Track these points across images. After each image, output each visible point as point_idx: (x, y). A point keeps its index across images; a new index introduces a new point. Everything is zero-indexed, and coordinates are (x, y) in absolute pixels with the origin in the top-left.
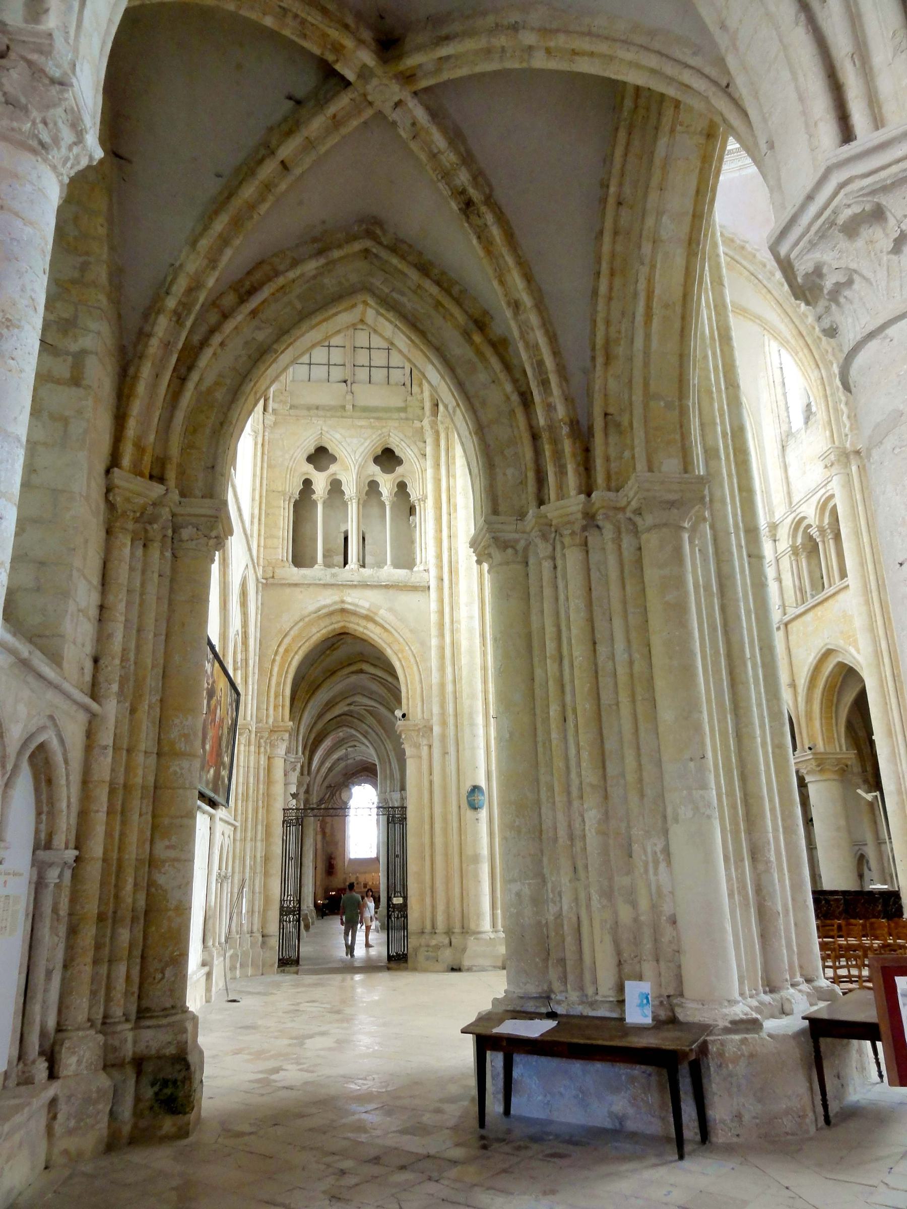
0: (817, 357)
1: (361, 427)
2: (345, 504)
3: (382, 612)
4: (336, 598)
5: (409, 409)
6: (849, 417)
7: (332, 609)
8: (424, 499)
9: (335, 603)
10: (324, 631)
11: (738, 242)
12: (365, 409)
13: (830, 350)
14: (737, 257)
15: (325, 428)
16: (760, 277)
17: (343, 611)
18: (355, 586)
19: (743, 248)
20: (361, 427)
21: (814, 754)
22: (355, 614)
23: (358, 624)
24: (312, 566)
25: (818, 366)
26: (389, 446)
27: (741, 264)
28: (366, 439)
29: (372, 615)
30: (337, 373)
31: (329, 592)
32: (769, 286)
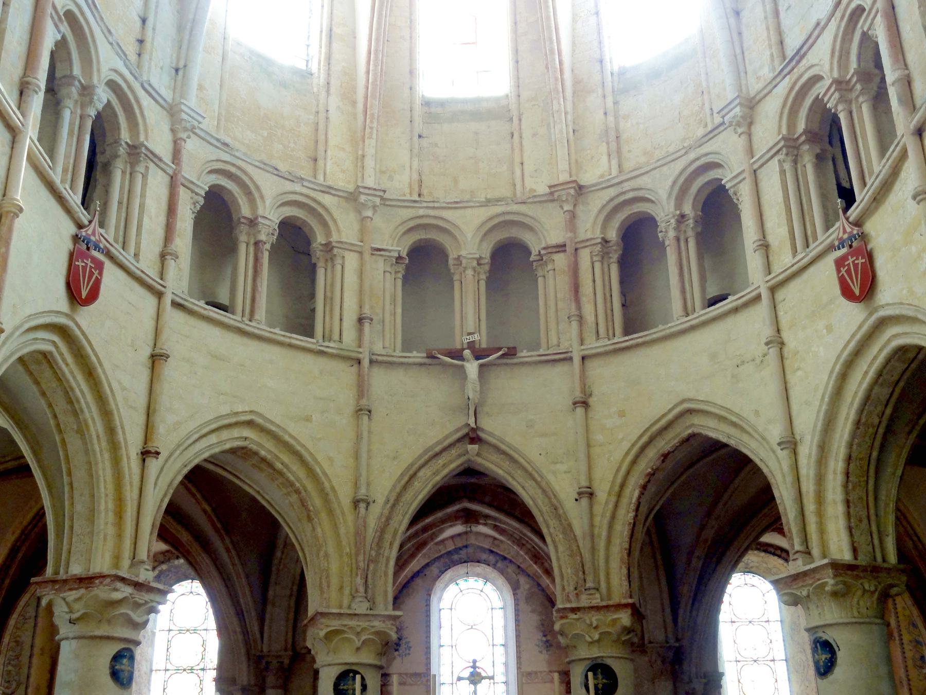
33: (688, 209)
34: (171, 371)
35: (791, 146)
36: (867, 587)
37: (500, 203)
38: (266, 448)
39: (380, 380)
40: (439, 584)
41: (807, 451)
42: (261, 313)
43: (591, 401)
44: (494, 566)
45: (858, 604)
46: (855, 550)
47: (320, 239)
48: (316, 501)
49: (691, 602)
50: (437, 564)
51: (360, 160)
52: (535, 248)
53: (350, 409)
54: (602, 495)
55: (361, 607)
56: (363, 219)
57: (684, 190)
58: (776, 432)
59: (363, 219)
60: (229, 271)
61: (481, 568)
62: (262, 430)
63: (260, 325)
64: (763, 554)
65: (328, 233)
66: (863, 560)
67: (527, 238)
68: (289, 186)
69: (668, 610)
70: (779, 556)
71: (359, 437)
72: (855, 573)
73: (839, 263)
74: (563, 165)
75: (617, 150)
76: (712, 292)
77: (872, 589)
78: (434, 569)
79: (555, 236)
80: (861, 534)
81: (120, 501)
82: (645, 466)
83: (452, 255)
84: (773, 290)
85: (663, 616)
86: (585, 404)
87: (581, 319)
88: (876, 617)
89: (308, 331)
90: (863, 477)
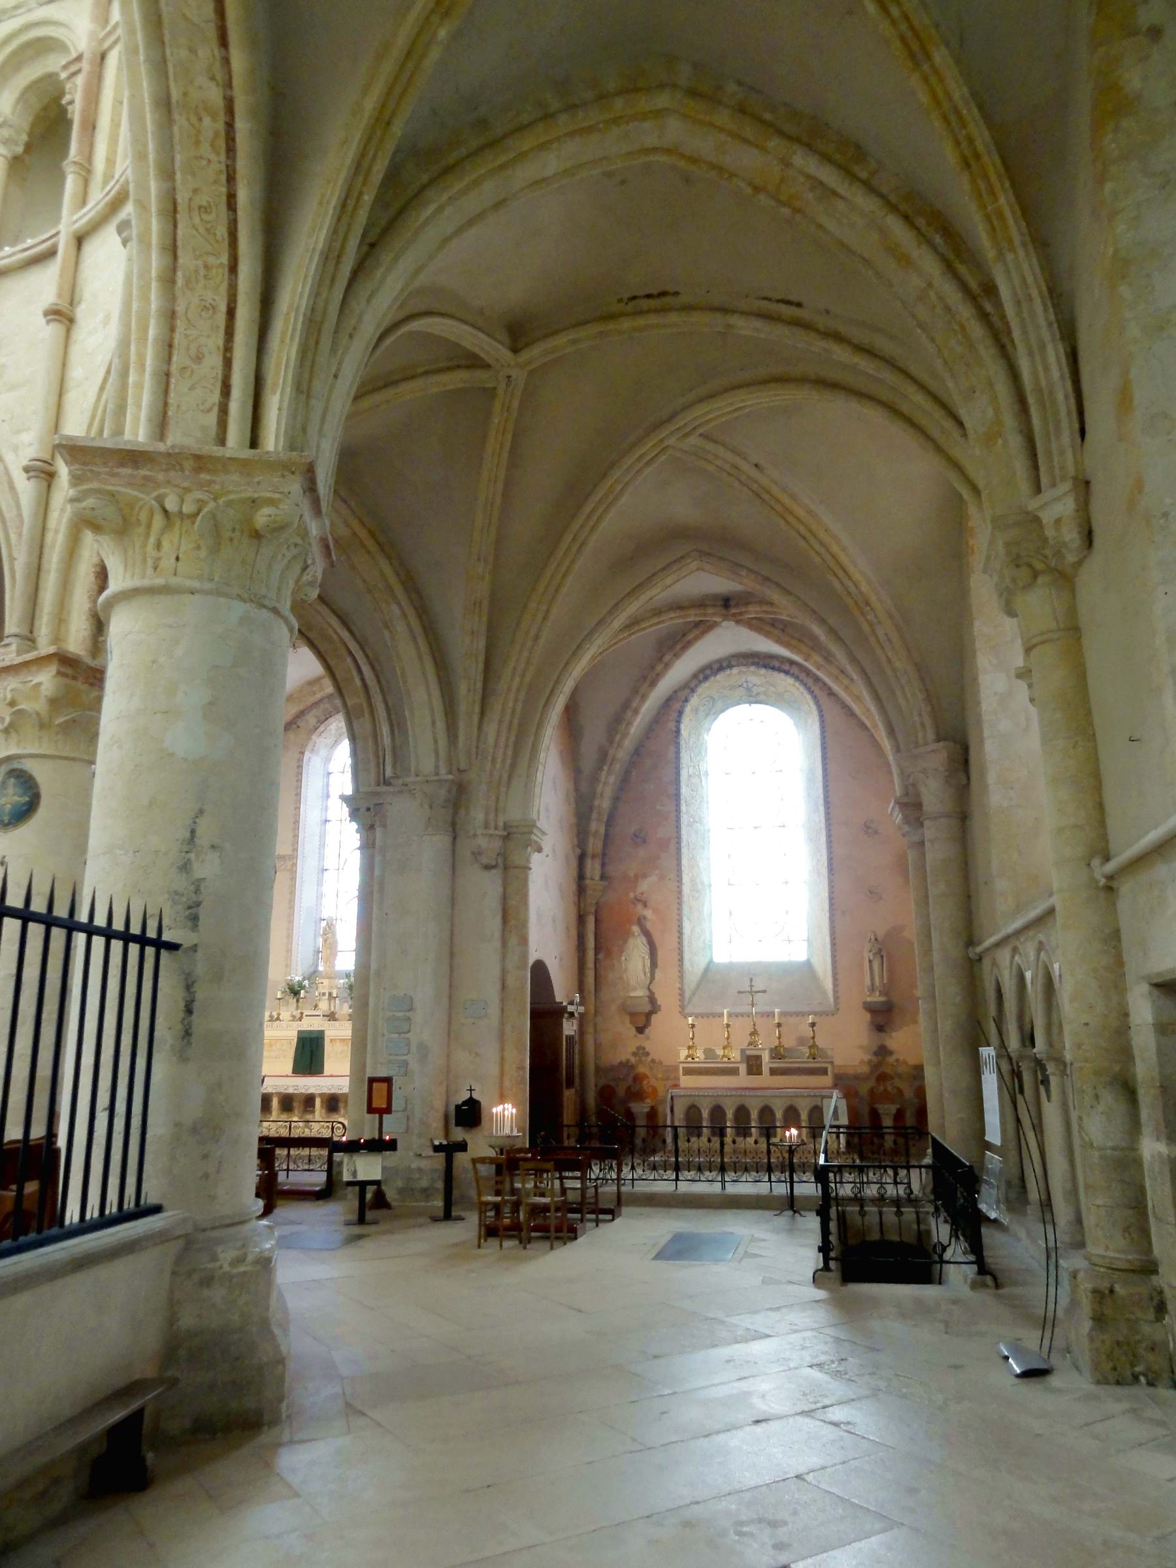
36: (171, 504)
37: (19, 11)
43: (81, 312)
45: (158, 546)
49: (477, 709)
50: (314, 711)
64: (763, 671)
69: (441, 725)
70: (787, 673)
72: (143, 472)
77: (188, 508)
78: (311, 719)
80: (191, 388)
85: (434, 733)
88: (199, 578)
90: (216, 255)
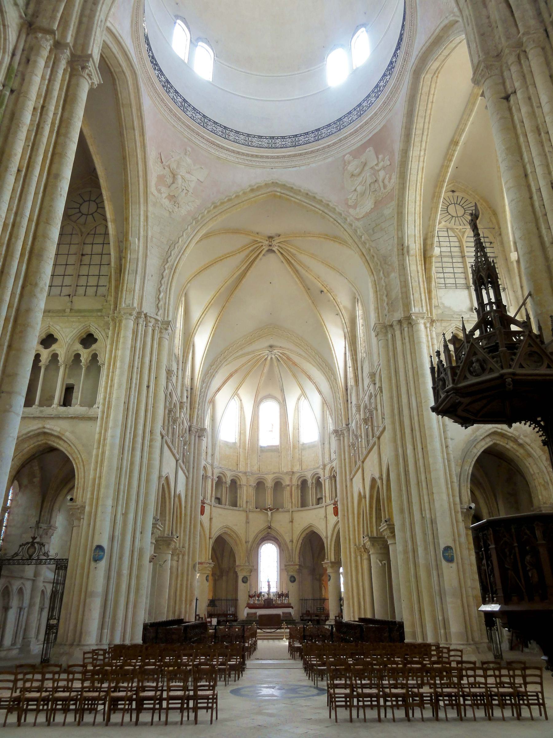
0: (372, 268)
1: (73, 322)
2: (58, 369)
3: (67, 434)
4: (40, 426)
5: (104, 310)
6: (387, 304)
7: (36, 432)
8: (104, 364)
9: (39, 429)
10: (32, 446)
11: (324, 201)
12: (79, 311)
13: (379, 264)
14: (326, 211)
15: (51, 323)
16: (339, 221)
17: (45, 433)
18: (53, 418)
19: (328, 205)
20: (73, 322)
21: (388, 525)
22: (52, 435)
23: (54, 442)
24: (31, 407)
25: (373, 273)
26: (91, 332)
27: (328, 215)
28: (75, 329)
29: (60, 435)
30: (66, 291)
31: (36, 422)
32: (345, 227)
33: (314, 481)
34: (214, 520)
35: (330, 478)
38: (229, 532)
39: (251, 515)
40: (261, 546)
41: (329, 539)
42: (227, 504)
44: (275, 541)
46: (335, 559)
47: (238, 483)
48: (238, 542)
51: (247, 464)
52: (284, 484)
53: (245, 522)
54: (294, 541)
55: (247, 564)
56: (248, 478)
57: (313, 477)
58: (325, 534)
59: (248, 478)
60: (220, 490)
61: (272, 541)
62: (228, 528)
63: (227, 507)
65: (240, 482)
66: (337, 560)
67: (282, 481)
68: (232, 473)
71: (247, 528)
73: (334, 508)
74: (290, 467)
75: (301, 464)
76: (319, 496)
79: (288, 483)
81: (206, 547)
82: (303, 536)
83: (266, 485)
84: (326, 506)
86: (292, 522)
87: (292, 503)
89: (236, 506)
